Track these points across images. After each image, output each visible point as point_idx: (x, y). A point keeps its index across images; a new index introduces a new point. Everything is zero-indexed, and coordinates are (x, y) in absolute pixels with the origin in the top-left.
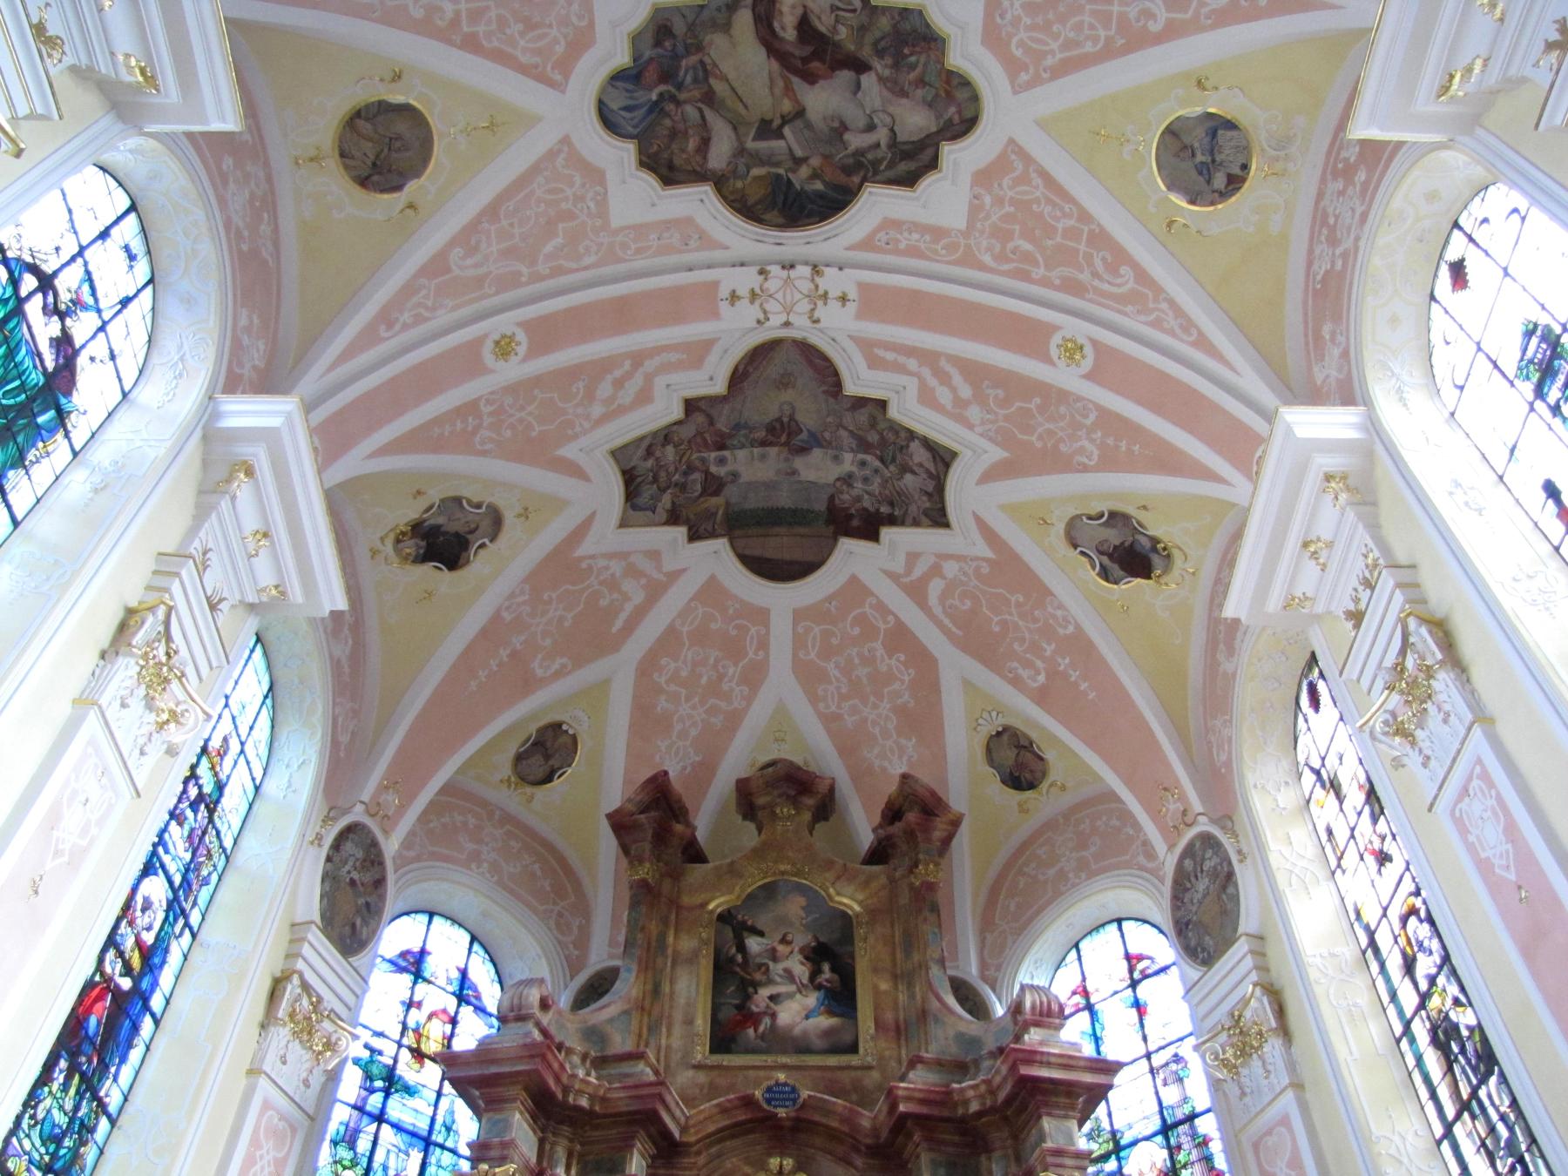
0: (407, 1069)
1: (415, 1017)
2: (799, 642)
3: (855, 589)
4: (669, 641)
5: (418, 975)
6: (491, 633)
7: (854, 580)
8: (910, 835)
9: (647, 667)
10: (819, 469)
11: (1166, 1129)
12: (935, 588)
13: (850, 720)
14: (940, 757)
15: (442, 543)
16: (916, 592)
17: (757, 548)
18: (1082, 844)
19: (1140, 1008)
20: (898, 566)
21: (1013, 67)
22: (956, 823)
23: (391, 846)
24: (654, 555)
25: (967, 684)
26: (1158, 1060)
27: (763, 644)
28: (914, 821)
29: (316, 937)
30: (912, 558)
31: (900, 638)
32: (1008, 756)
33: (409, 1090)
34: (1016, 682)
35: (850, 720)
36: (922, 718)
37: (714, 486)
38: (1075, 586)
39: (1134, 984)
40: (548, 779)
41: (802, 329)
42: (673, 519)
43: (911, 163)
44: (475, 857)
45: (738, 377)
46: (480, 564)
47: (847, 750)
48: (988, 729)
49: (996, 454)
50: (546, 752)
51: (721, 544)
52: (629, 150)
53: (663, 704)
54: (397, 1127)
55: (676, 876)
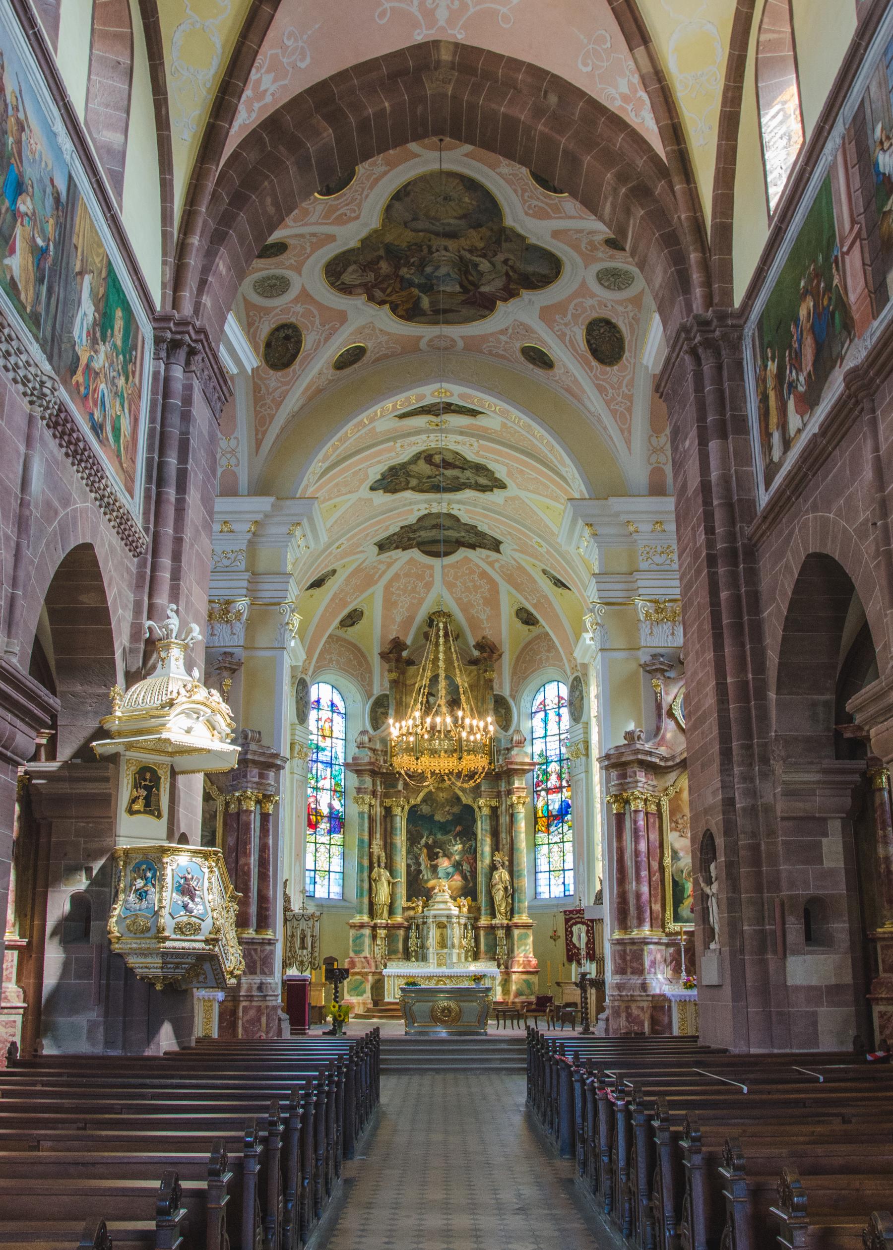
0: (321, 744)
1: (320, 723)
2: (444, 575)
3: (467, 559)
4: (396, 577)
5: (319, 709)
6: (332, 600)
7: (466, 558)
8: (485, 659)
9: (387, 587)
10: (453, 534)
11: (560, 761)
12: (497, 565)
13: (465, 600)
14: (498, 615)
15: (318, 583)
16: (491, 564)
17: (428, 548)
18: (548, 651)
19: (559, 715)
20: (484, 556)
21: (517, 484)
22: (500, 656)
23: (308, 679)
24: (390, 557)
25: (509, 593)
26: (562, 737)
27: (432, 576)
28: (488, 652)
29: (299, 727)
30: (488, 557)
31: (484, 575)
32: (525, 616)
33: (323, 750)
34: (526, 599)
35: (465, 600)
36: (493, 601)
37: (410, 539)
38: (546, 585)
39: (559, 708)
40: (352, 625)
41: (445, 511)
42: (397, 548)
43: (483, 489)
44: (331, 661)
45: (421, 519)
46: (328, 584)
47: (464, 610)
48: (516, 607)
49: (516, 547)
50: (353, 618)
51: (416, 550)
52: (381, 491)
53: (394, 598)
54: (322, 762)
55: (403, 673)
